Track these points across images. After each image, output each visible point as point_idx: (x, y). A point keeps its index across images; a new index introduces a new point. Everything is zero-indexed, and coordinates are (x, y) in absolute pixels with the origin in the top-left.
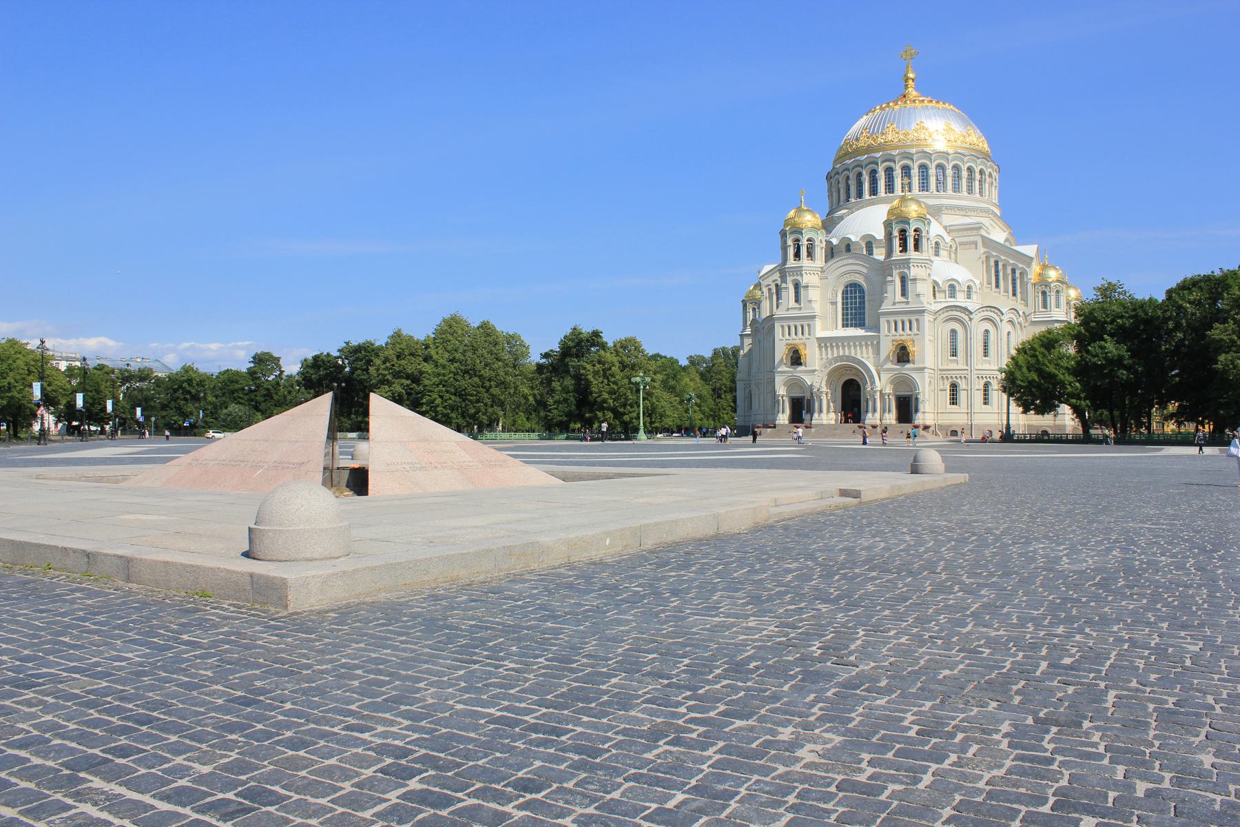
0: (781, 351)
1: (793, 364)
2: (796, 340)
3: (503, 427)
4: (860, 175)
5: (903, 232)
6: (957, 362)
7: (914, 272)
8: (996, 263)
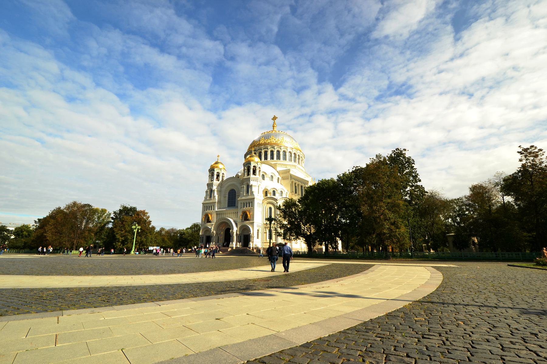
7: (252, 183)
8: (295, 184)
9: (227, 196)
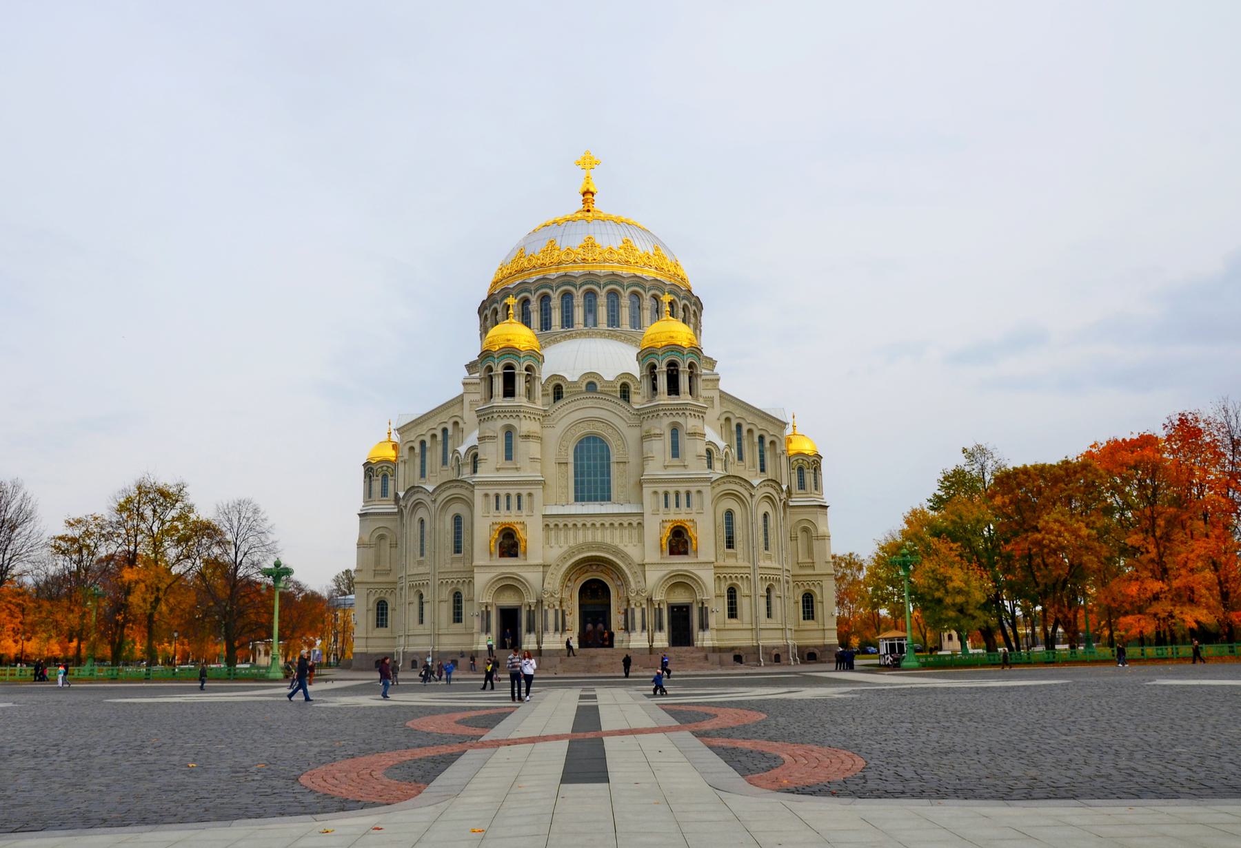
0: (483, 531)
1: (502, 554)
2: (508, 517)
3: (788, 652)
4: (545, 298)
5: (673, 364)
6: (735, 556)
7: (691, 424)
9: (571, 460)
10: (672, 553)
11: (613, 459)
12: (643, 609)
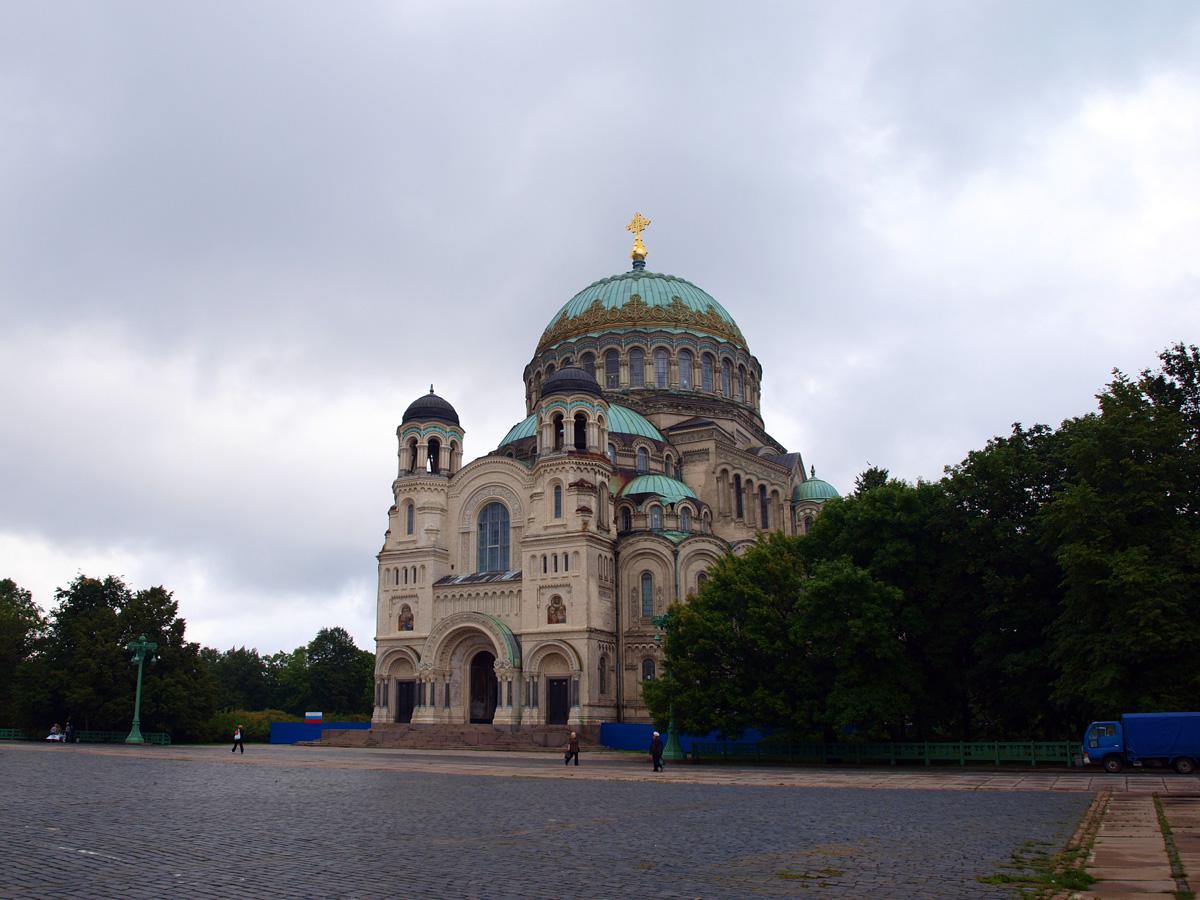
9: (474, 527)
10: (550, 621)
11: (511, 525)
12: (510, 683)
